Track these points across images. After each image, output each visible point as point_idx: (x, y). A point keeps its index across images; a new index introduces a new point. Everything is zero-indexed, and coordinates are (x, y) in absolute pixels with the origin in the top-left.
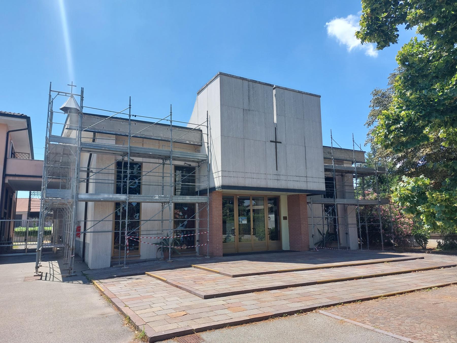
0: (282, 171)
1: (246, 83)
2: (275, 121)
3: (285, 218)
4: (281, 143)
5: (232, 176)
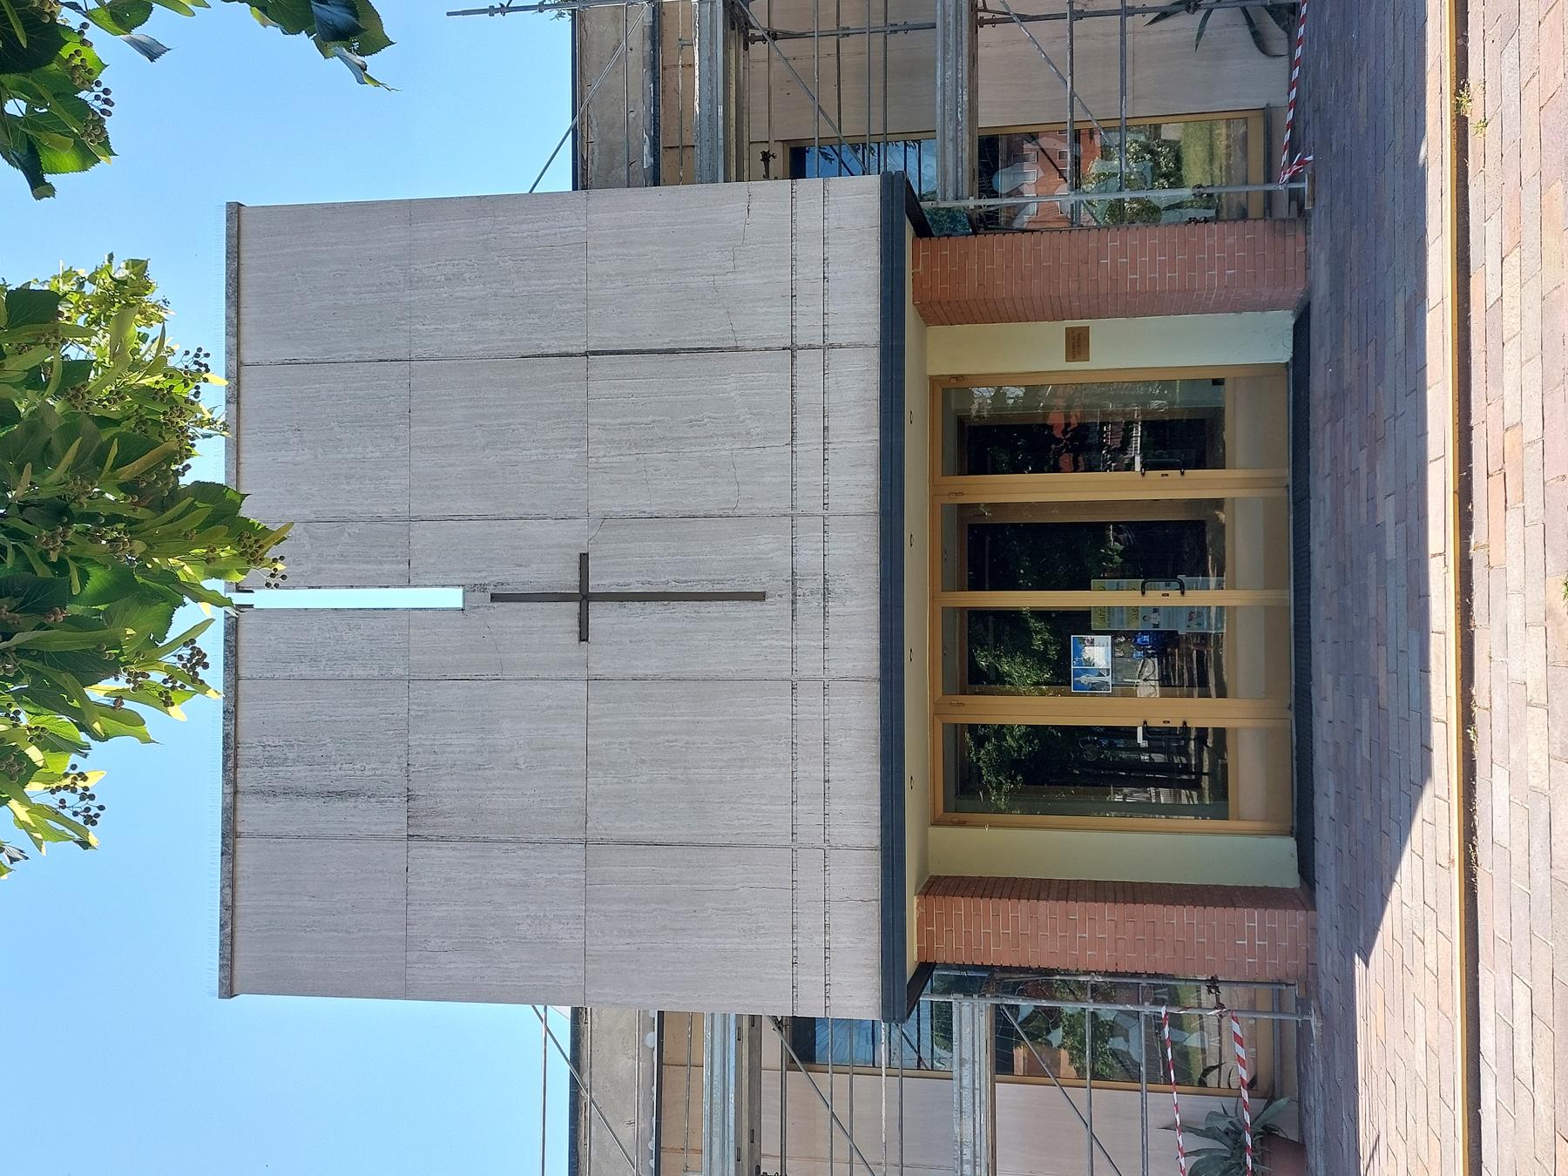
0: (760, 554)
1: (249, 809)
2: (452, 598)
3: (1077, 344)
4: (584, 558)
5: (819, 939)
